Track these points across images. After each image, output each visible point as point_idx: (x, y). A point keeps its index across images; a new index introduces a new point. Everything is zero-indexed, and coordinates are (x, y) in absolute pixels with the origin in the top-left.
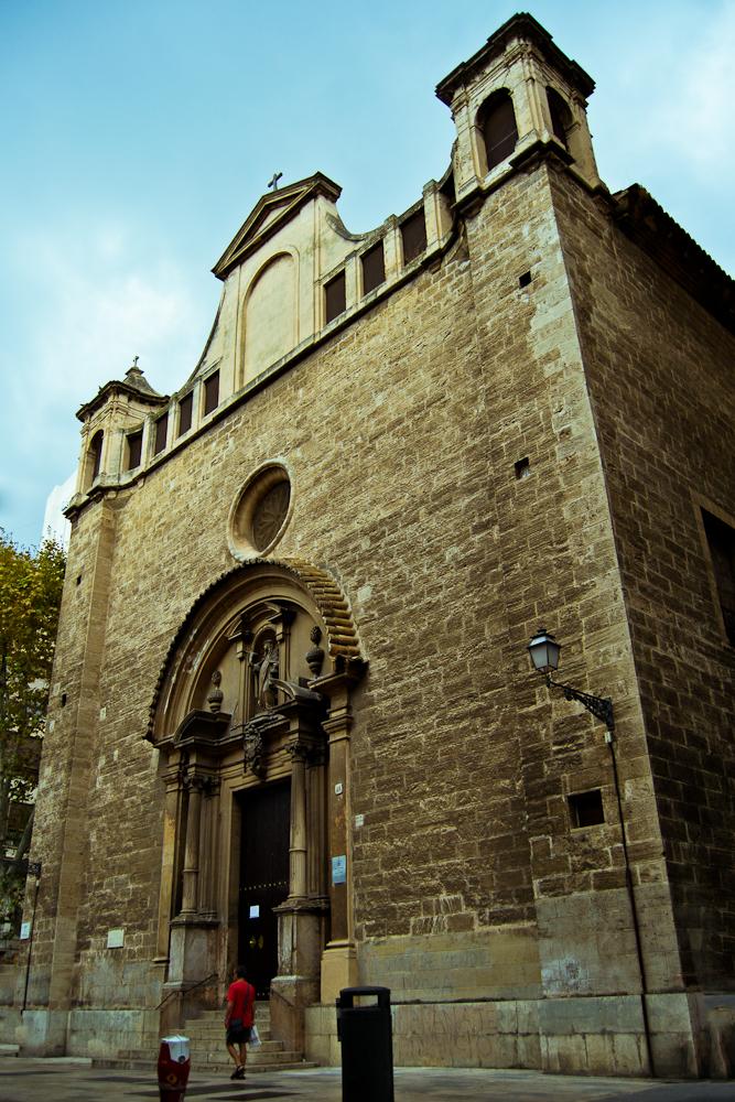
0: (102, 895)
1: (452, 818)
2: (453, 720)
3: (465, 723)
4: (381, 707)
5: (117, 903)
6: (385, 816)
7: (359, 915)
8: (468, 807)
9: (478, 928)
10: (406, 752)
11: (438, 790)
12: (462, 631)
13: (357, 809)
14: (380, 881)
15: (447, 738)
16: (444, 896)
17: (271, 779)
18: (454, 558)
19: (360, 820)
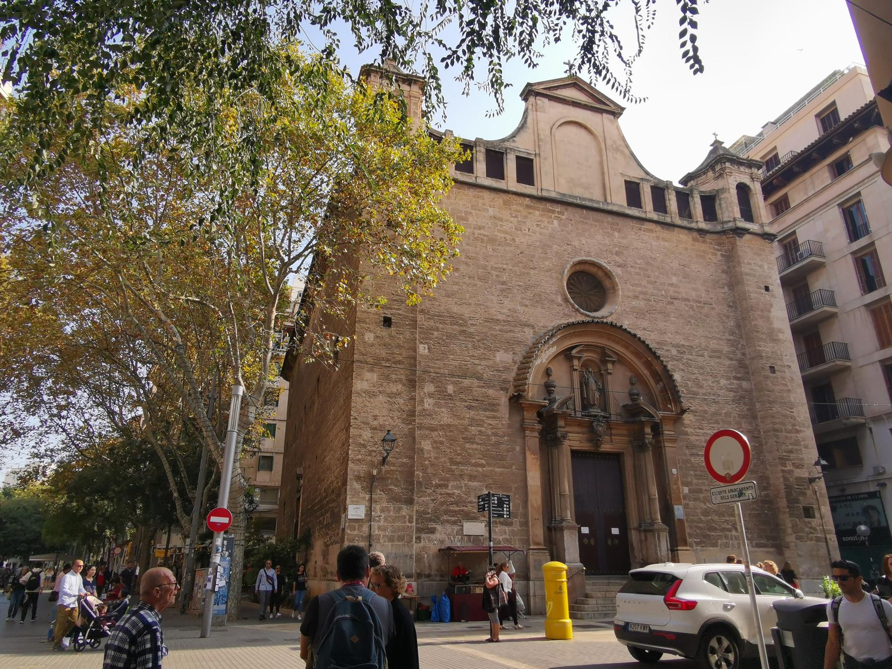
0: (448, 494)
4: (693, 438)
6: (700, 491)
7: (691, 535)
12: (731, 419)
13: (686, 484)
14: (701, 522)
18: (725, 385)
19: (686, 490)
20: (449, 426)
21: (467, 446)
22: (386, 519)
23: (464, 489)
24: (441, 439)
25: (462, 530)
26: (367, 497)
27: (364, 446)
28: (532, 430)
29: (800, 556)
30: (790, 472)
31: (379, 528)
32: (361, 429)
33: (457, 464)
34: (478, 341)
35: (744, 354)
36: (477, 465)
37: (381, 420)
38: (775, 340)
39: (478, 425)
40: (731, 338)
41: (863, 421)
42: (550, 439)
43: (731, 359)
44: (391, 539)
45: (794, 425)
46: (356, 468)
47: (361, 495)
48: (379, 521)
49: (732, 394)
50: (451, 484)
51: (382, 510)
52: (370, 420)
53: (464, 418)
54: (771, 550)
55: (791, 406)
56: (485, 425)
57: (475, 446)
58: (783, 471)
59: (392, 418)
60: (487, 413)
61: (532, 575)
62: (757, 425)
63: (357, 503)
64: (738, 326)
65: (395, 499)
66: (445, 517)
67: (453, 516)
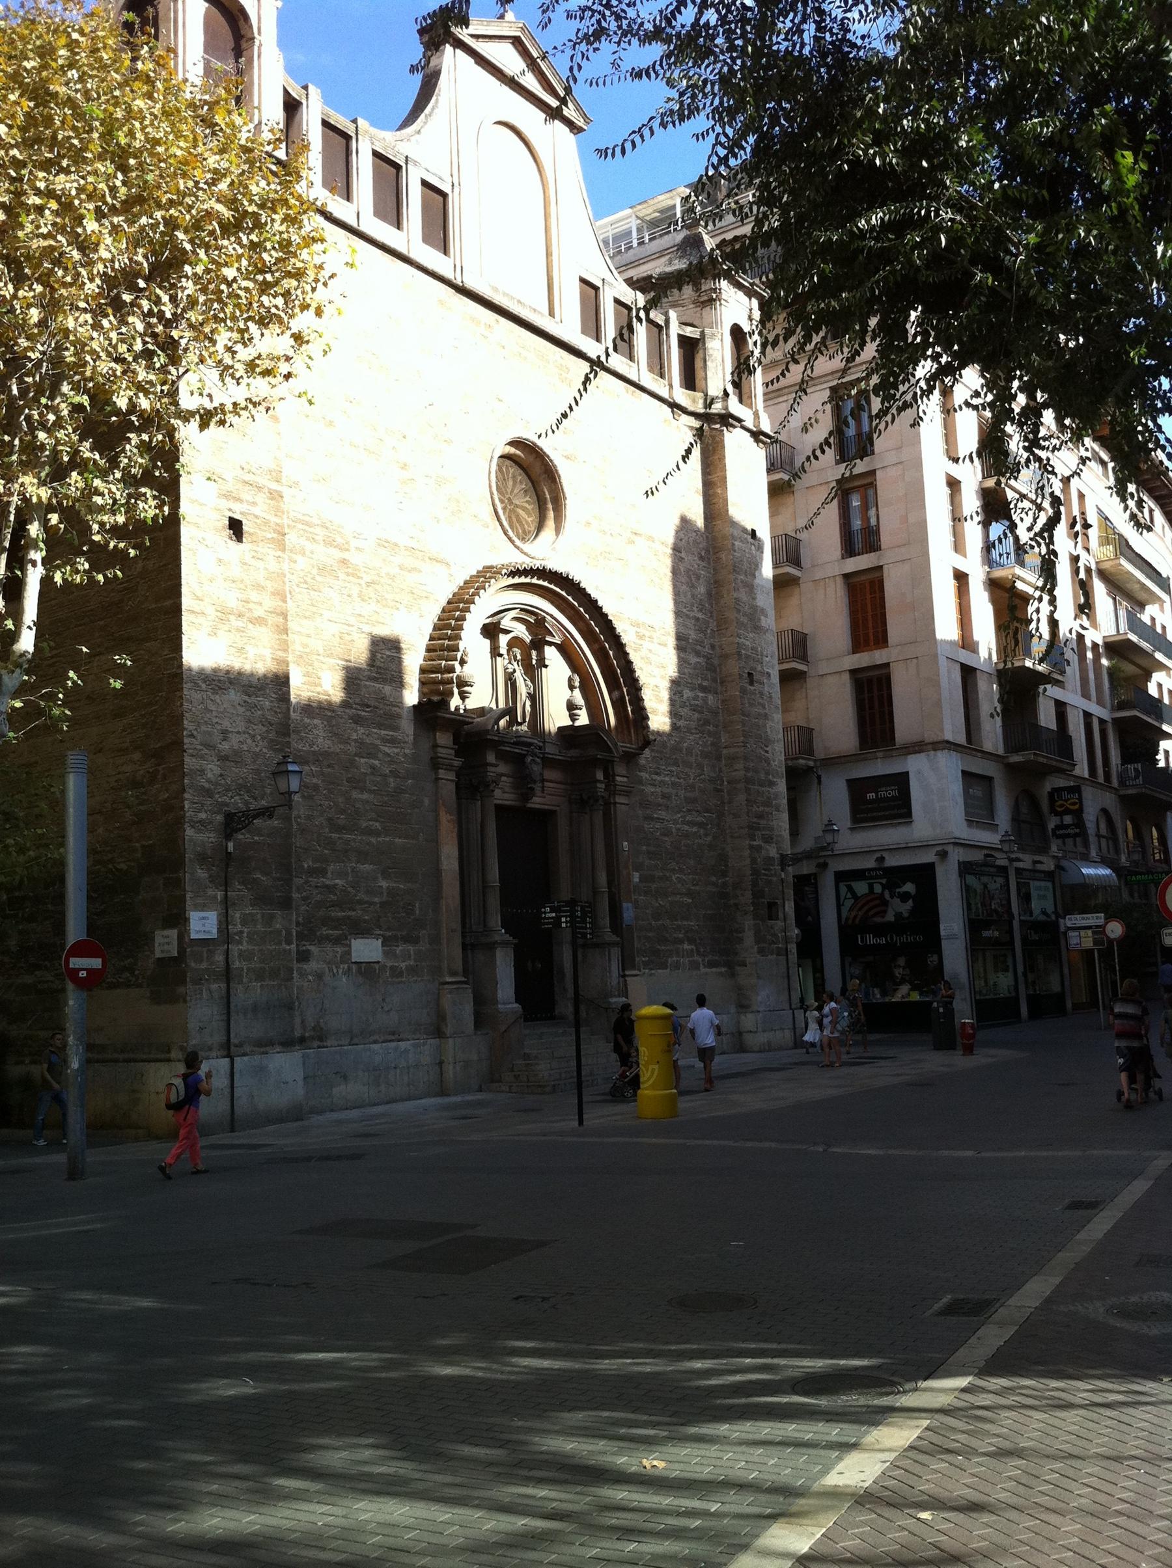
0: (327, 887)
1: (689, 894)
2: (690, 823)
3: (695, 829)
5: (360, 902)
8: (697, 888)
9: (703, 970)
10: (665, 835)
11: (681, 871)
15: (687, 835)
16: (686, 946)
17: (533, 806)
19: (636, 877)
20: (326, 754)
21: (355, 794)
22: (251, 939)
23: (350, 879)
24: (315, 780)
25: (349, 953)
26: (220, 895)
27: (209, 793)
28: (449, 768)
29: (759, 977)
30: (758, 849)
31: (240, 955)
32: (202, 758)
33: (339, 829)
34: (368, 584)
35: (713, 647)
36: (370, 832)
37: (234, 740)
38: (757, 628)
39: (370, 755)
40: (700, 615)
41: (811, 763)
42: (471, 785)
43: (698, 654)
44: (260, 976)
45: (767, 773)
46: (200, 837)
47: (210, 892)
48: (240, 942)
49: (697, 715)
50: (331, 868)
51: (244, 922)
52: (217, 738)
53: (346, 742)
54: (723, 970)
55: (767, 742)
56: (380, 755)
57: (365, 796)
58: (751, 847)
59: (253, 737)
60: (383, 732)
61: (449, 1030)
62: (720, 771)
63: (203, 908)
64: (709, 594)
65: (261, 900)
66: (325, 931)
67: (335, 928)
